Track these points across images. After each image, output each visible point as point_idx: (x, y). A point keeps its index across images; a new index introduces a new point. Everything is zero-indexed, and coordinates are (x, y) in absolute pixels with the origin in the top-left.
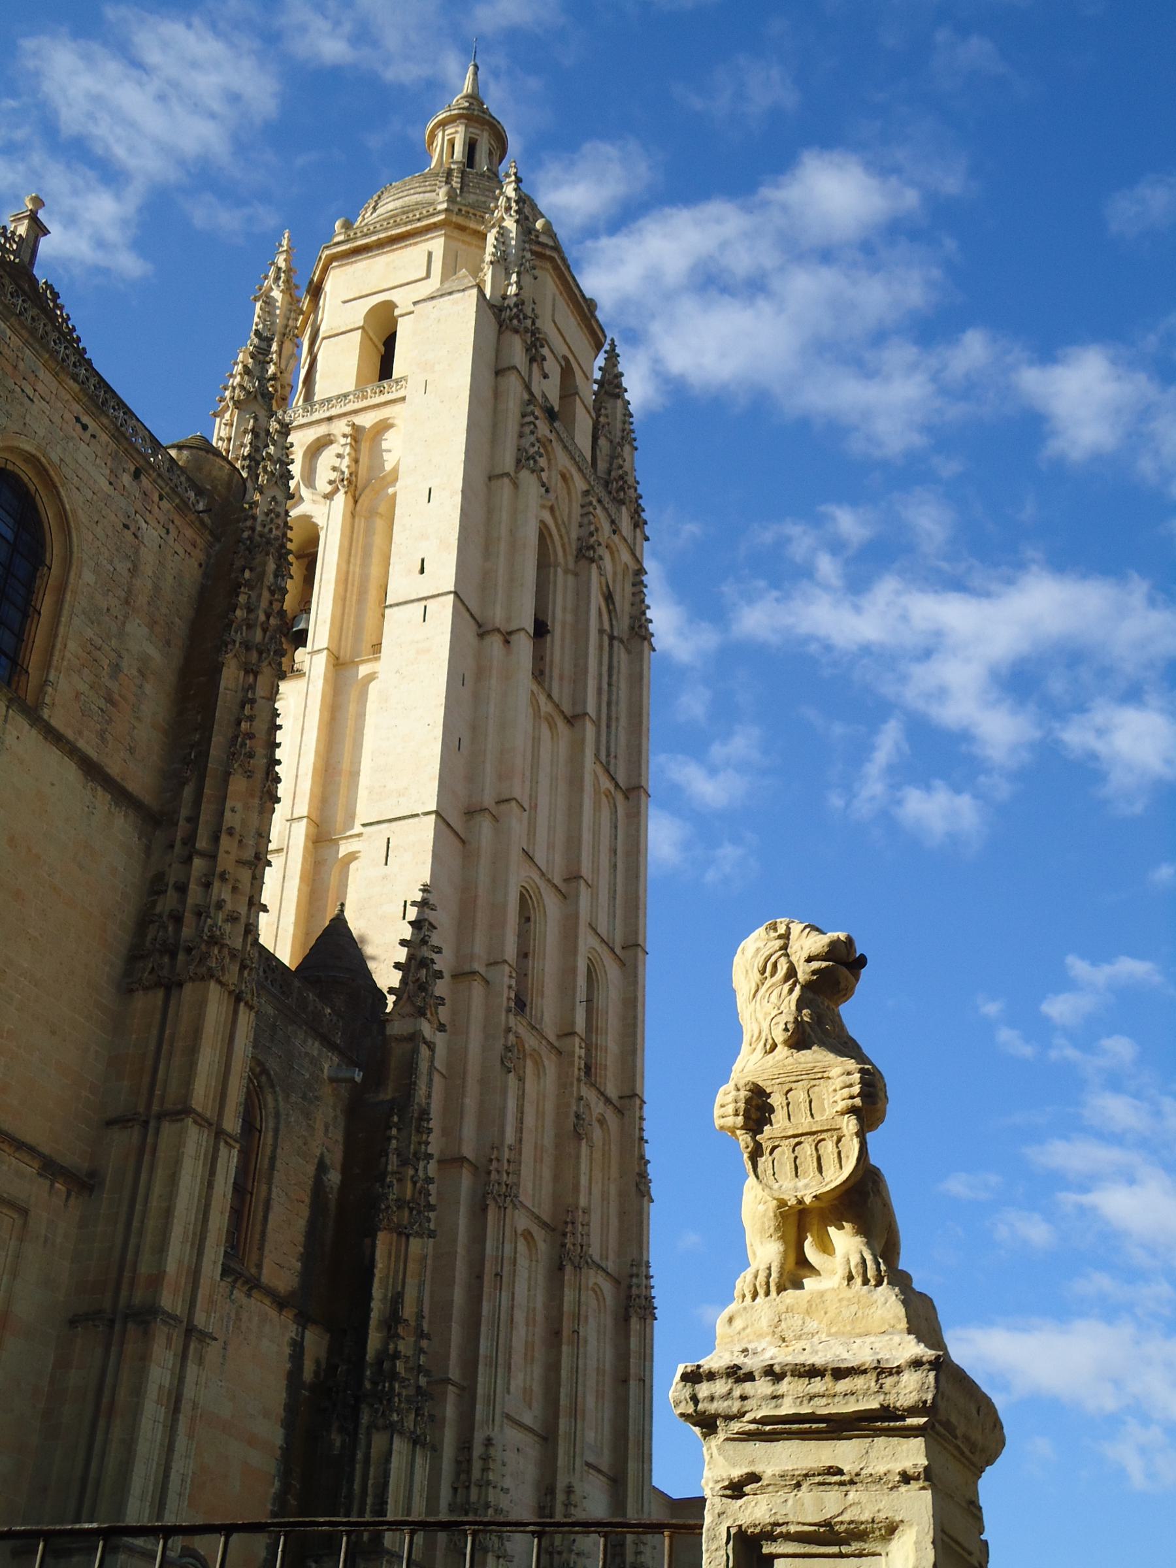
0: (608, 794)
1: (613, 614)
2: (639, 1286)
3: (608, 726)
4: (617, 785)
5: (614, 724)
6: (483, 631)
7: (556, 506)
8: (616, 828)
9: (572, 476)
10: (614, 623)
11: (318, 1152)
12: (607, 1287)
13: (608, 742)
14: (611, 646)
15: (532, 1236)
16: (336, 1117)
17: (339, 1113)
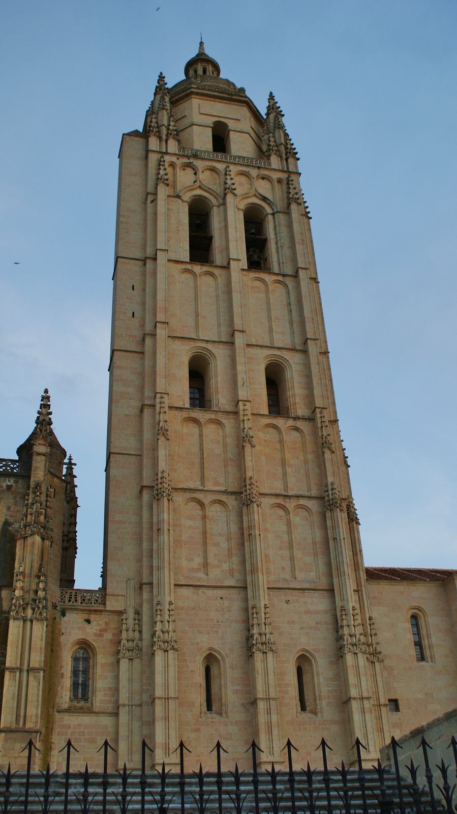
0: (279, 282)
1: (271, 204)
2: (328, 496)
3: (278, 252)
4: (284, 275)
5: (280, 250)
6: (144, 261)
7: (201, 185)
8: (289, 293)
9: (214, 167)
10: (273, 207)
11: (3, 519)
12: (313, 505)
13: (279, 259)
14: (274, 218)
15: (222, 501)
16: (16, 502)
17: (18, 499)
